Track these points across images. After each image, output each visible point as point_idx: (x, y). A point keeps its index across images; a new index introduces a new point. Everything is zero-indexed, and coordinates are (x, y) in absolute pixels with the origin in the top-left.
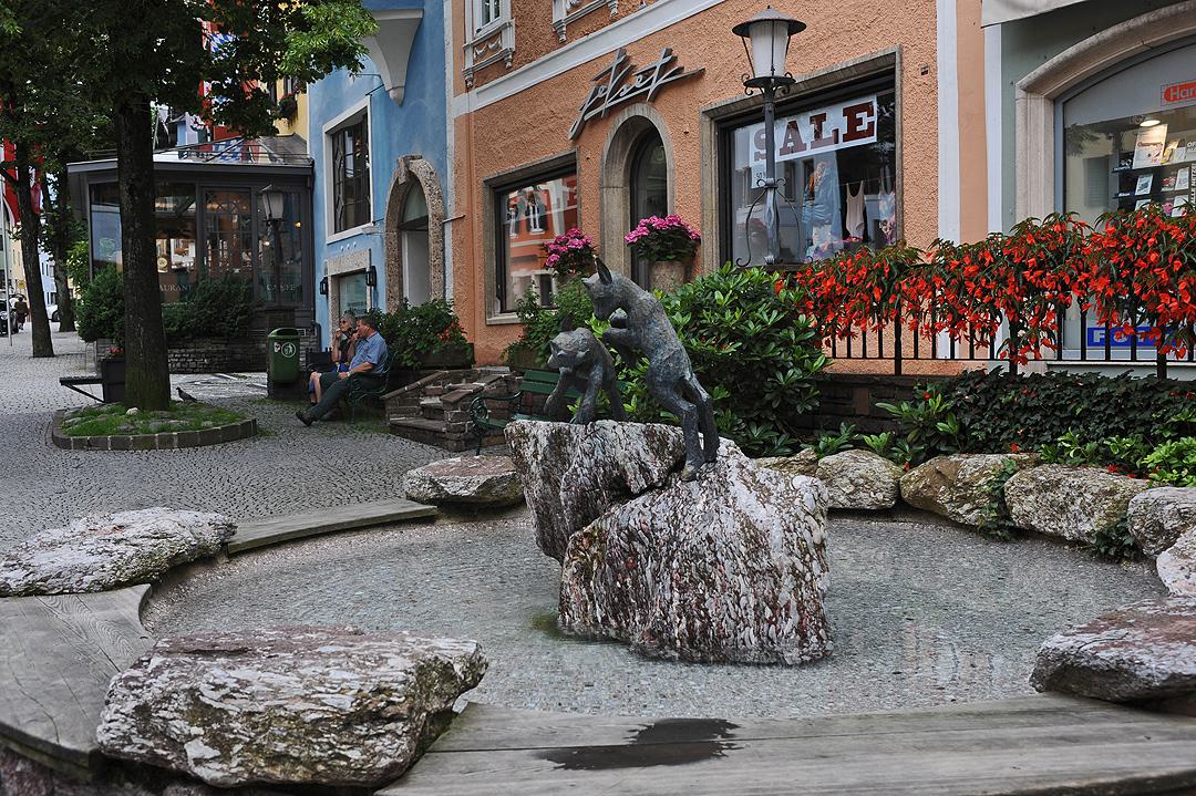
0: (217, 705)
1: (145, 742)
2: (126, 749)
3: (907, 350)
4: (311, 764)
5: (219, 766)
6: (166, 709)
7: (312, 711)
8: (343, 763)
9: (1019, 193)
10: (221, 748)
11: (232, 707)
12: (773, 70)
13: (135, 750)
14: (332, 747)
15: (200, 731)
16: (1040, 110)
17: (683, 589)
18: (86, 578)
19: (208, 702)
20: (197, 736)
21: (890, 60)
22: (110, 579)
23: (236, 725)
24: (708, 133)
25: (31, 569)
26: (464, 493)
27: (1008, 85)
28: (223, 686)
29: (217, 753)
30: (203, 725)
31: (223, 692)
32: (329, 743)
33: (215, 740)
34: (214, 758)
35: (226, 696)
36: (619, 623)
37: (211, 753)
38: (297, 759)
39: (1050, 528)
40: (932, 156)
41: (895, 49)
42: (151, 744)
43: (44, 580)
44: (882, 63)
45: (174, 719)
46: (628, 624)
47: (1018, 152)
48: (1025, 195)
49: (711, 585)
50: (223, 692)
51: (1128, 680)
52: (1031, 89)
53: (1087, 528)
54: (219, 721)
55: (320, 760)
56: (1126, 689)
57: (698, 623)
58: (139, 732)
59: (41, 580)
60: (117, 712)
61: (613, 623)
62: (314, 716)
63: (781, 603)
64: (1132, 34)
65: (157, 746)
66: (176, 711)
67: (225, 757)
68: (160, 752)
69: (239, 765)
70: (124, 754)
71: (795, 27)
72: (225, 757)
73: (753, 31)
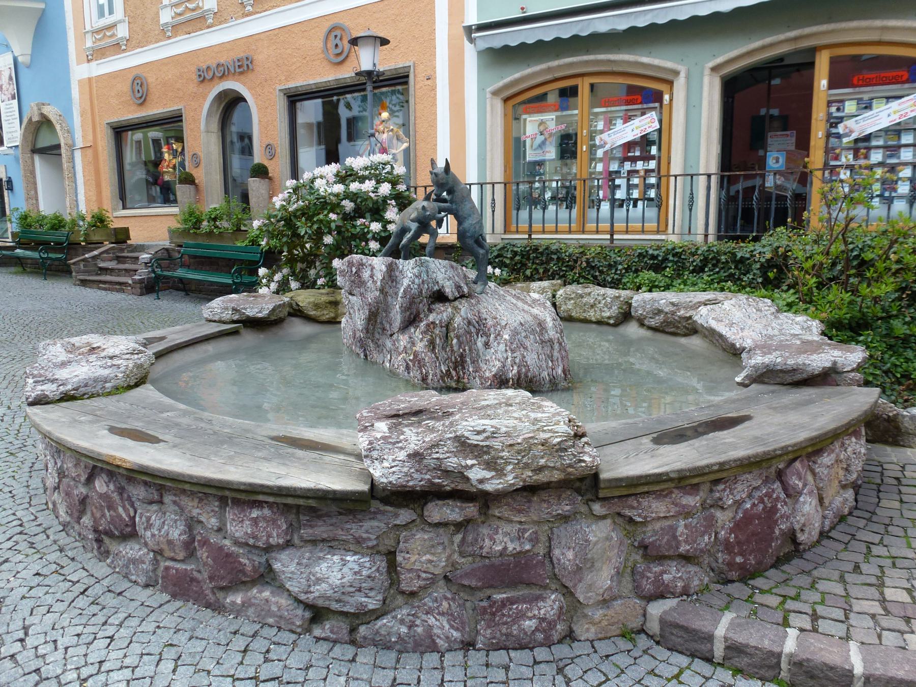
0: (484, 444)
1: (423, 476)
2: (411, 484)
3: (537, 226)
4: (563, 469)
5: (498, 482)
6: (437, 453)
7: (556, 437)
8: (583, 464)
9: (488, 148)
10: (495, 470)
11: (497, 444)
12: (374, 65)
13: (416, 483)
14: (575, 456)
15: (474, 462)
16: (499, 104)
17: (513, 351)
18: (108, 385)
19: (476, 443)
20: (473, 465)
21: (406, 70)
22: (120, 382)
23: (505, 454)
24: (281, 105)
25: (60, 383)
26: (260, 315)
27: (481, 90)
28: (484, 431)
29: (493, 473)
30: (476, 457)
31: (485, 435)
32: (573, 454)
33: (490, 465)
34: (492, 477)
35: (487, 438)
36: (457, 373)
37: (488, 474)
38: (553, 468)
39: (583, 316)
40: (433, 125)
41: (411, 64)
42: (428, 477)
43: (76, 389)
44: (401, 71)
45: (449, 457)
46: (464, 374)
47: (488, 130)
48: (492, 150)
49: (525, 348)
50: (485, 435)
51: (802, 373)
52: (495, 93)
53: (608, 314)
54: (487, 453)
55: (570, 466)
56: (798, 377)
57: (524, 370)
58: (417, 471)
59: (74, 389)
60: (394, 460)
61: (454, 373)
62: (559, 440)
63: (555, 359)
64: (549, 69)
65: (434, 477)
66: (447, 452)
67: (500, 473)
68: (437, 481)
69: (514, 478)
70: (410, 487)
71: (384, 42)
72: (500, 473)
73: (360, 42)
